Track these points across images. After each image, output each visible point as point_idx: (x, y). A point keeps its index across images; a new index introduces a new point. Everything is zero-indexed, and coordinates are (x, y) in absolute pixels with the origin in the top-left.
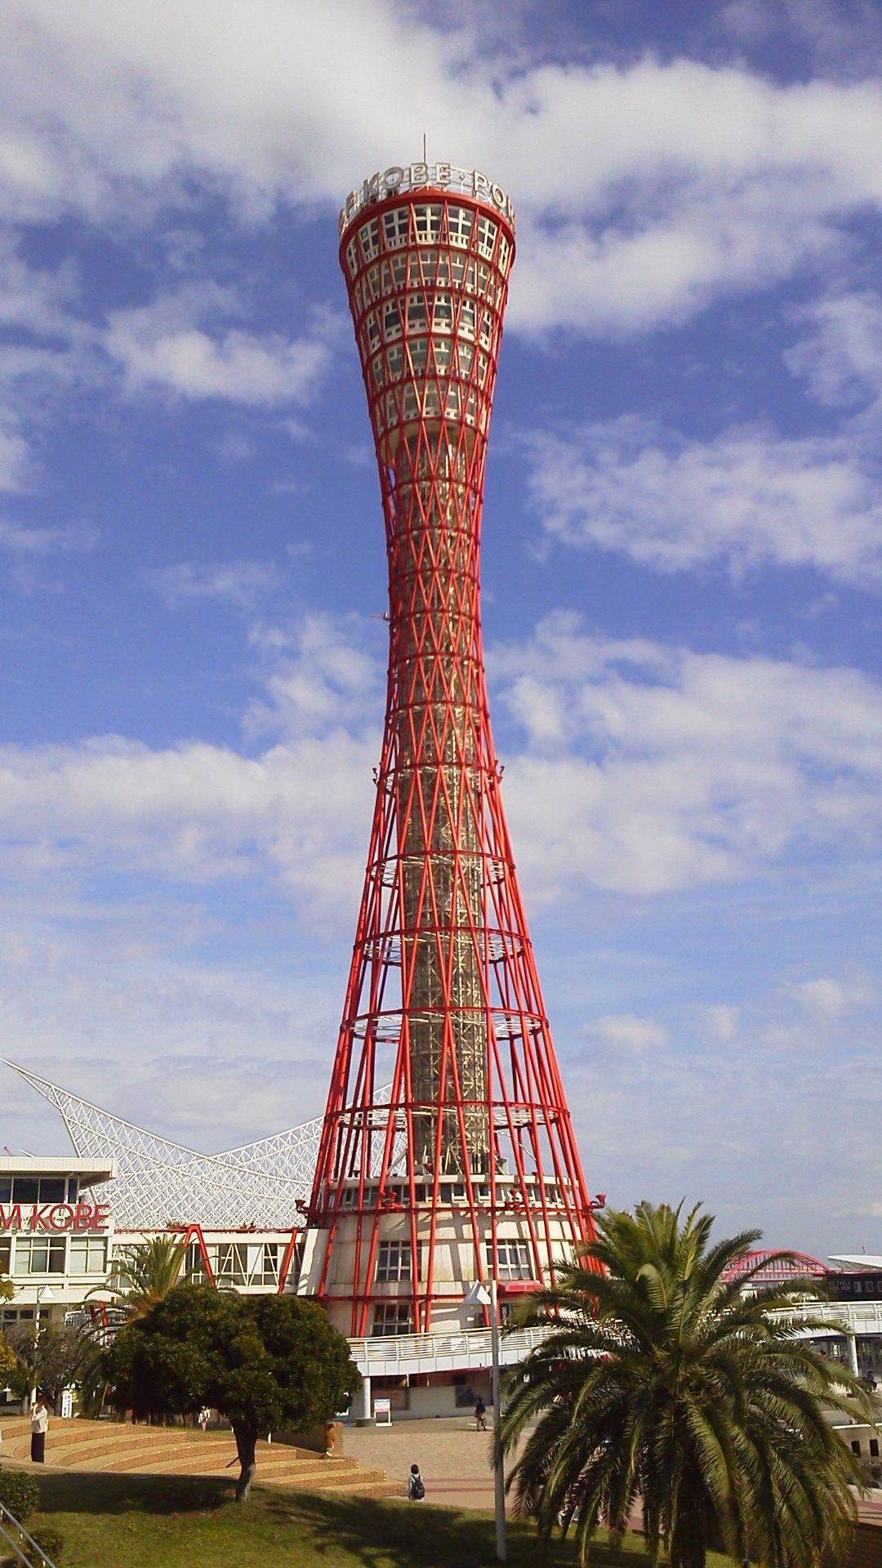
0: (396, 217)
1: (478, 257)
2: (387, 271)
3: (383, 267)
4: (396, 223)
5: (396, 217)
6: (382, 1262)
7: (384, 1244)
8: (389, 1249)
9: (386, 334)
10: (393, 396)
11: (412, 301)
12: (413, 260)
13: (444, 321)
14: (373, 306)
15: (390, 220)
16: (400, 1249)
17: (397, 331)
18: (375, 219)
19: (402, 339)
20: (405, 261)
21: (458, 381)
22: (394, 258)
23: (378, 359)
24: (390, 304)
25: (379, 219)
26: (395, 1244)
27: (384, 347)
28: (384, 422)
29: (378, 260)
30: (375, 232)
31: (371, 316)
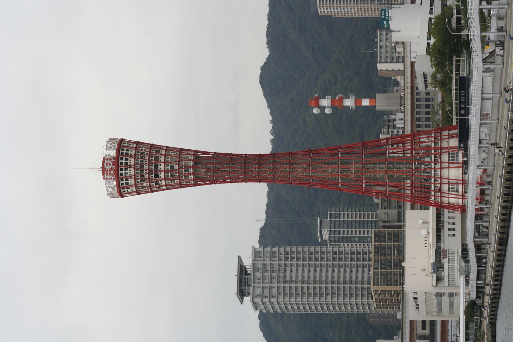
0: (122, 182)
1: (135, 155)
2: (140, 185)
3: (139, 186)
4: (124, 182)
5: (122, 182)
6: (454, 191)
7: (449, 191)
8: (450, 189)
9: (161, 185)
10: (183, 182)
11: (152, 177)
12: (138, 176)
13: (159, 167)
14: (151, 188)
15: (123, 184)
16: (450, 186)
17: (161, 181)
18: (121, 189)
19: (165, 179)
20: (138, 179)
21: (179, 162)
22: (136, 182)
23: (168, 187)
24: (151, 184)
25: (122, 187)
26: (449, 188)
27: (166, 185)
28: (191, 184)
29: (136, 187)
30: (125, 188)
31: (153, 189)
